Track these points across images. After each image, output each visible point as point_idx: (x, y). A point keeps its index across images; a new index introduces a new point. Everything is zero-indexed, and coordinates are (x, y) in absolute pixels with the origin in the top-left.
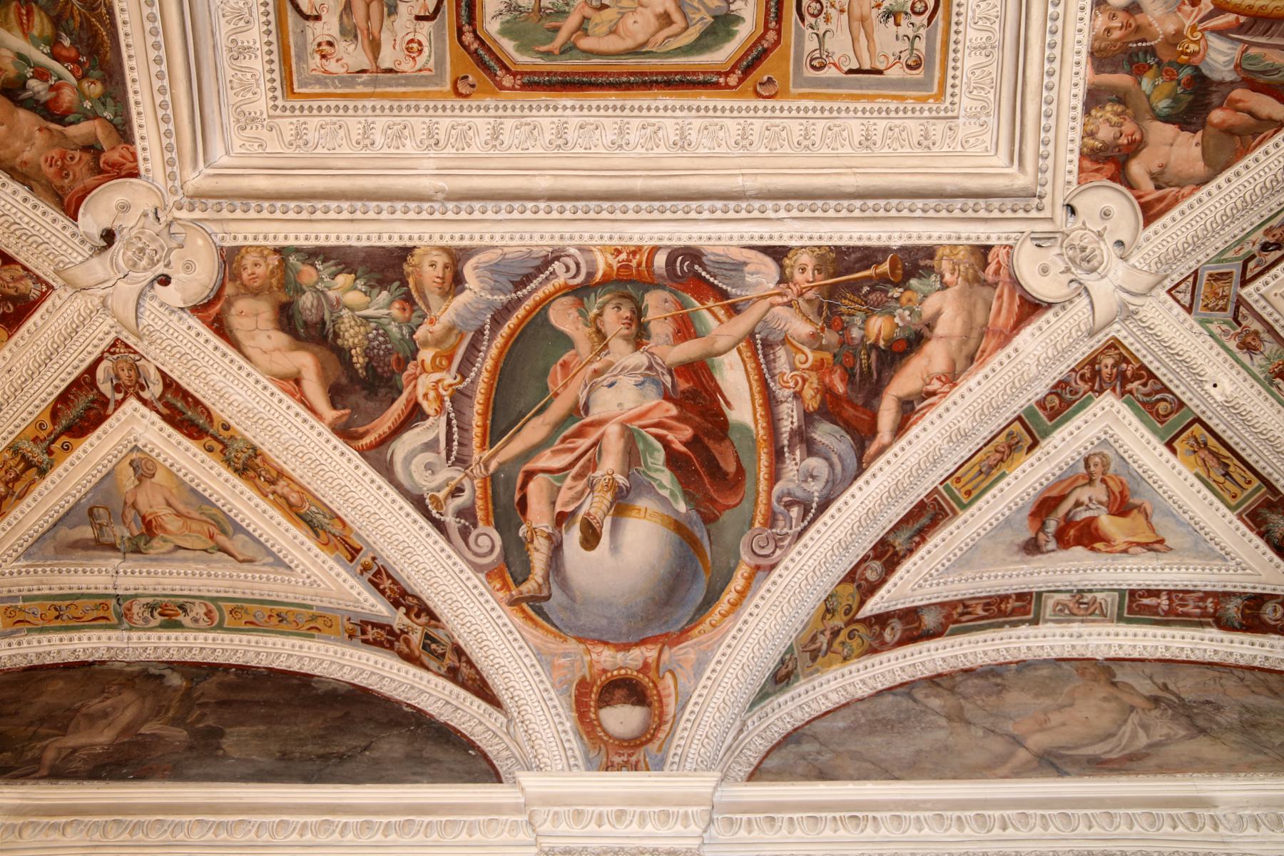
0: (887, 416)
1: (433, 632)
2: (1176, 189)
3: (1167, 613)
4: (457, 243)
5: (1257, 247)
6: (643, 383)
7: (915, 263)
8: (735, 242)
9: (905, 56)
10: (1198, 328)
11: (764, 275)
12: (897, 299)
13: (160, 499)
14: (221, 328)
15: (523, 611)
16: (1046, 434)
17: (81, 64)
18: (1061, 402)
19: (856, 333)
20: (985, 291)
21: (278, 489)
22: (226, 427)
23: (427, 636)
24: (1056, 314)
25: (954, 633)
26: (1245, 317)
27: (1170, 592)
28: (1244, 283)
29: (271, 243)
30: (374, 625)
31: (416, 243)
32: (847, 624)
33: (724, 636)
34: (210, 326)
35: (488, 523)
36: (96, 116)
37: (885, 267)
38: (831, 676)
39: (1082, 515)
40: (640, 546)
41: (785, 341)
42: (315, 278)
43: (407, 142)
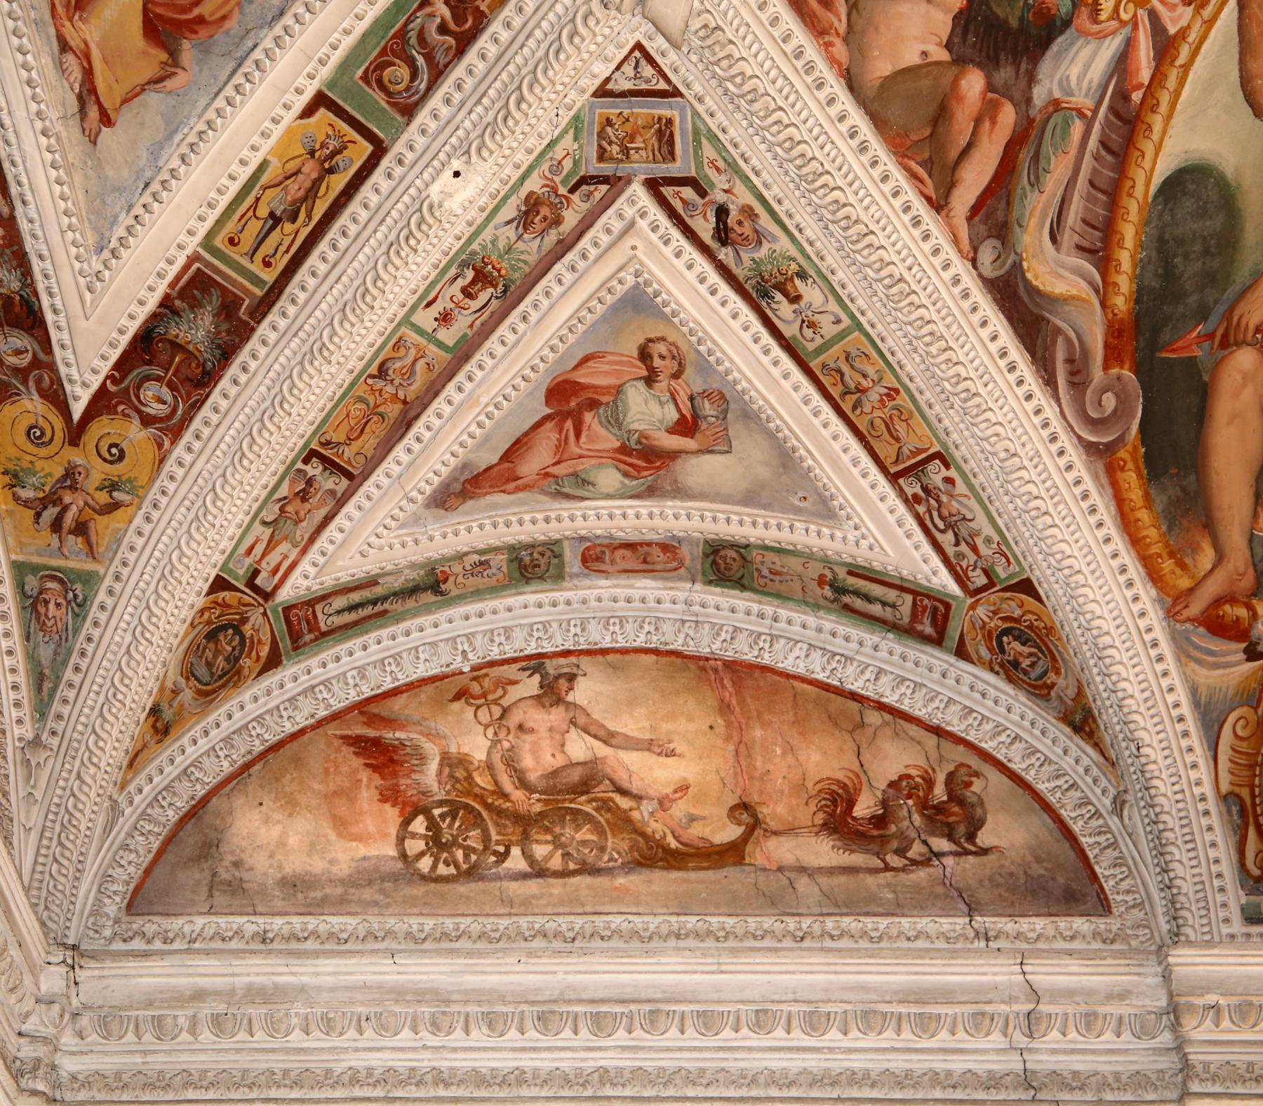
2: (842, 28)
5: (720, 197)
26: (589, 195)
28: (653, 185)
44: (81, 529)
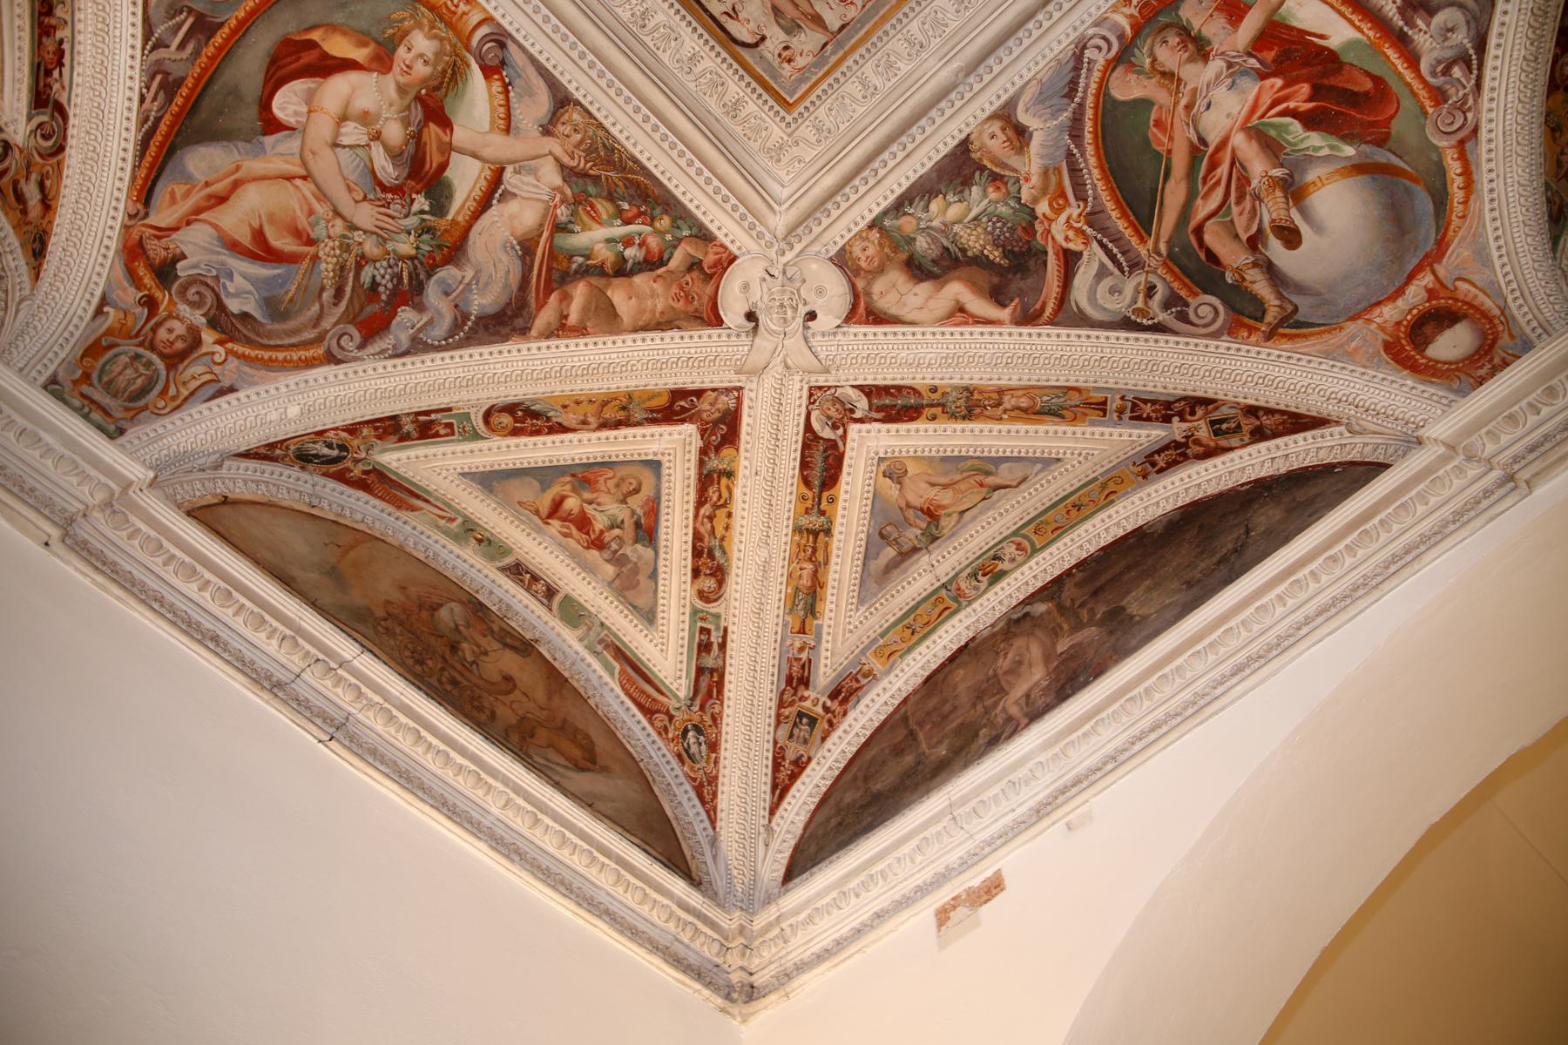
1: (1216, 415)
4: (997, 104)
13: (925, 486)
14: (877, 318)
15: (1284, 335)
17: (644, 213)
21: (1007, 405)
22: (934, 390)
23: (1213, 423)
29: (863, 224)
30: (1158, 452)
31: (967, 131)
33: (1481, 216)
34: (867, 323)
35: (1196, 295)
36: (680, 240)
42: (914, 222)
43: (899, 64)
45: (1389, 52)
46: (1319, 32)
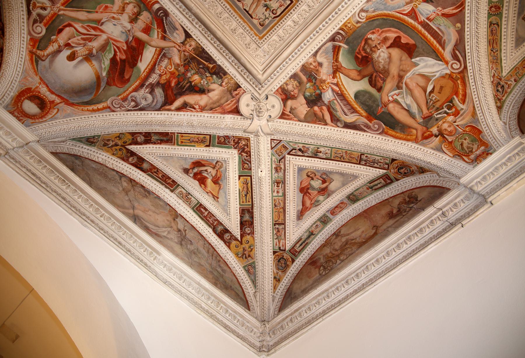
0: (178, 103)
3: (204, 217)
5: (298, 148)
6: (123, 33)
7: (219, 72)
8: (179, 21)
9: (261, 20)
10: (270, 154)
11: (179, 37)
12: (207, 77)
15: (32, 57)
16: (214, 146)
18: (224, 141)
19: (189, 75)
20: (230, 96)
24: (241, 119)
25: (149, 175)
27: (209, 212)
28: (289, 154)
32: (122, 146)
33: (83, 115)
37: (211, 66)
38: (105, 154)
39: (205, 174)
40: (83, 73)
41: (170, 59)
44: (249, 256)
45: (138, 82)
46: (142, 59)
